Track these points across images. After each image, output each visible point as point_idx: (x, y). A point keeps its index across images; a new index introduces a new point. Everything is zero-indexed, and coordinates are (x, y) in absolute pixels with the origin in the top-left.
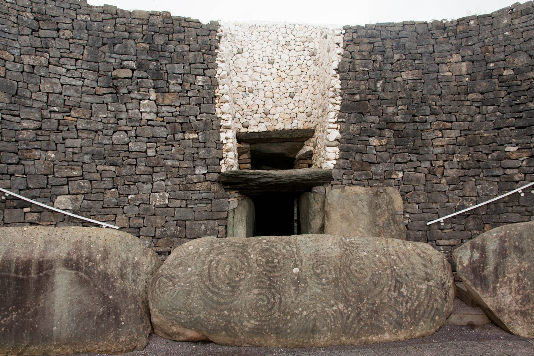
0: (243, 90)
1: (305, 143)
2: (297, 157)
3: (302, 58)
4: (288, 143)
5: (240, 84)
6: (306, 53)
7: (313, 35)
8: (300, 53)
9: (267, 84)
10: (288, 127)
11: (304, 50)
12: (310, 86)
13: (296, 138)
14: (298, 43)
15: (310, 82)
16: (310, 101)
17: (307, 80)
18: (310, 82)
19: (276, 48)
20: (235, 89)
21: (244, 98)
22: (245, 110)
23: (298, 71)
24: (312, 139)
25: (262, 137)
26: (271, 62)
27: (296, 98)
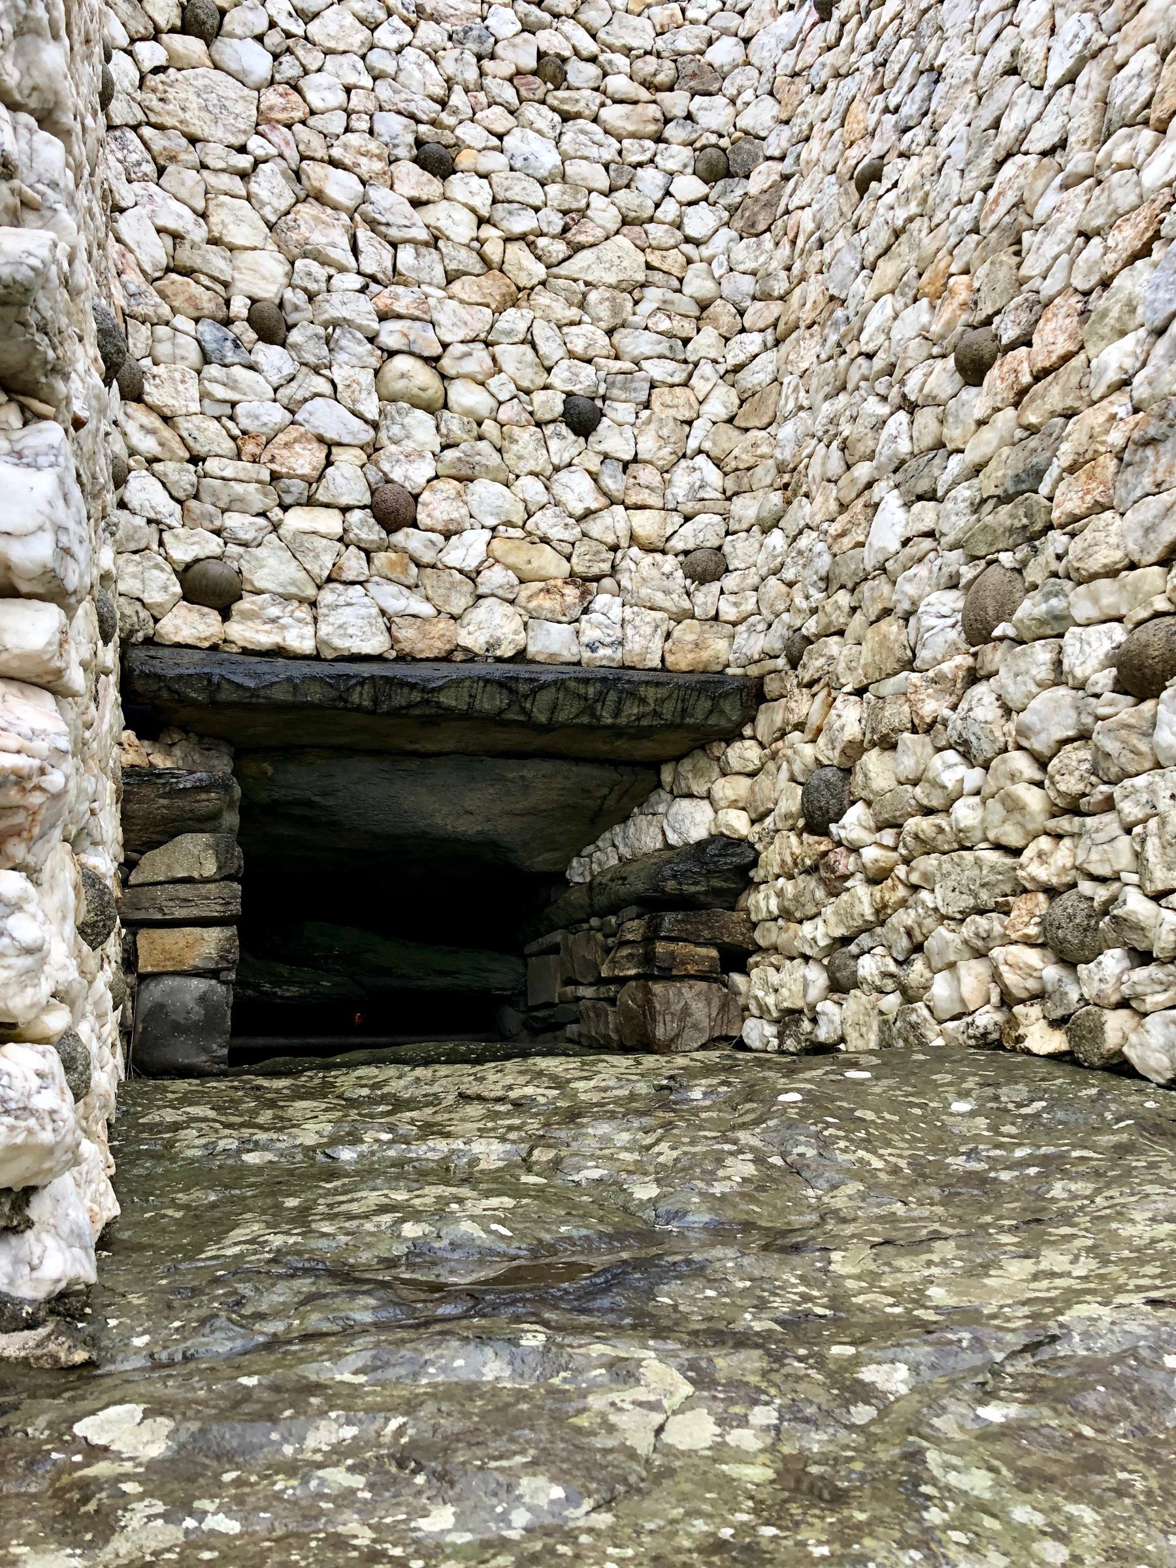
0: (208, 302)
1: (667, 776)
2: (578, 872)
3: (651, 180)
4: (547, 767)
5: (185, 256)
6: (676, 156)
7: (724, 52)
8: (635, 151)
9: (403, 299)
10: (553, 642)
11: (659, 139)
12: (706, 368)
13: (617, 732)
14: (618, 84)
15: (705, 342)
16: (713, 475)
17: (688, 328)
18: (705, 342)
19: (472, 75)
20: (134, 279)
21: (213, 370)
22: (212, 465)
23: (620, 258)
24: (744, 753)
25: (361, 697)
26: (438, 162)
27: (612, 438)
